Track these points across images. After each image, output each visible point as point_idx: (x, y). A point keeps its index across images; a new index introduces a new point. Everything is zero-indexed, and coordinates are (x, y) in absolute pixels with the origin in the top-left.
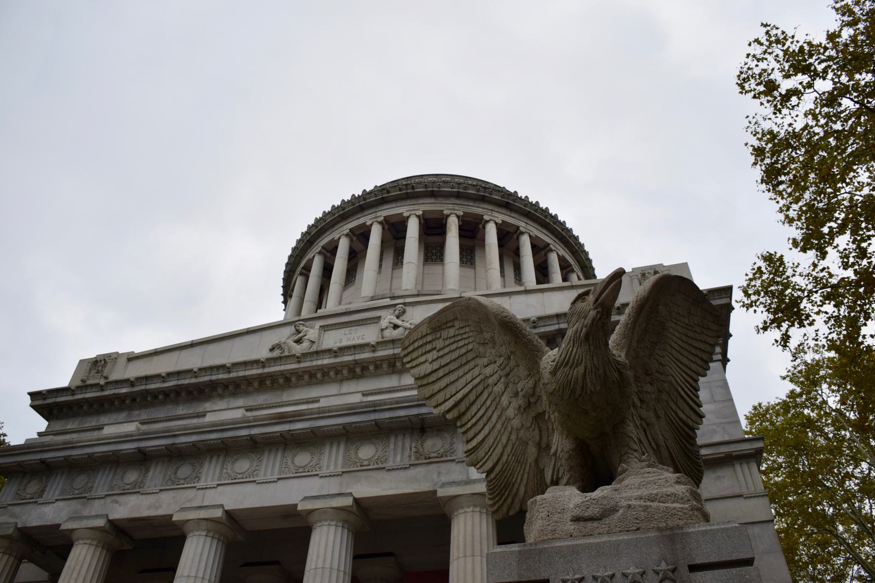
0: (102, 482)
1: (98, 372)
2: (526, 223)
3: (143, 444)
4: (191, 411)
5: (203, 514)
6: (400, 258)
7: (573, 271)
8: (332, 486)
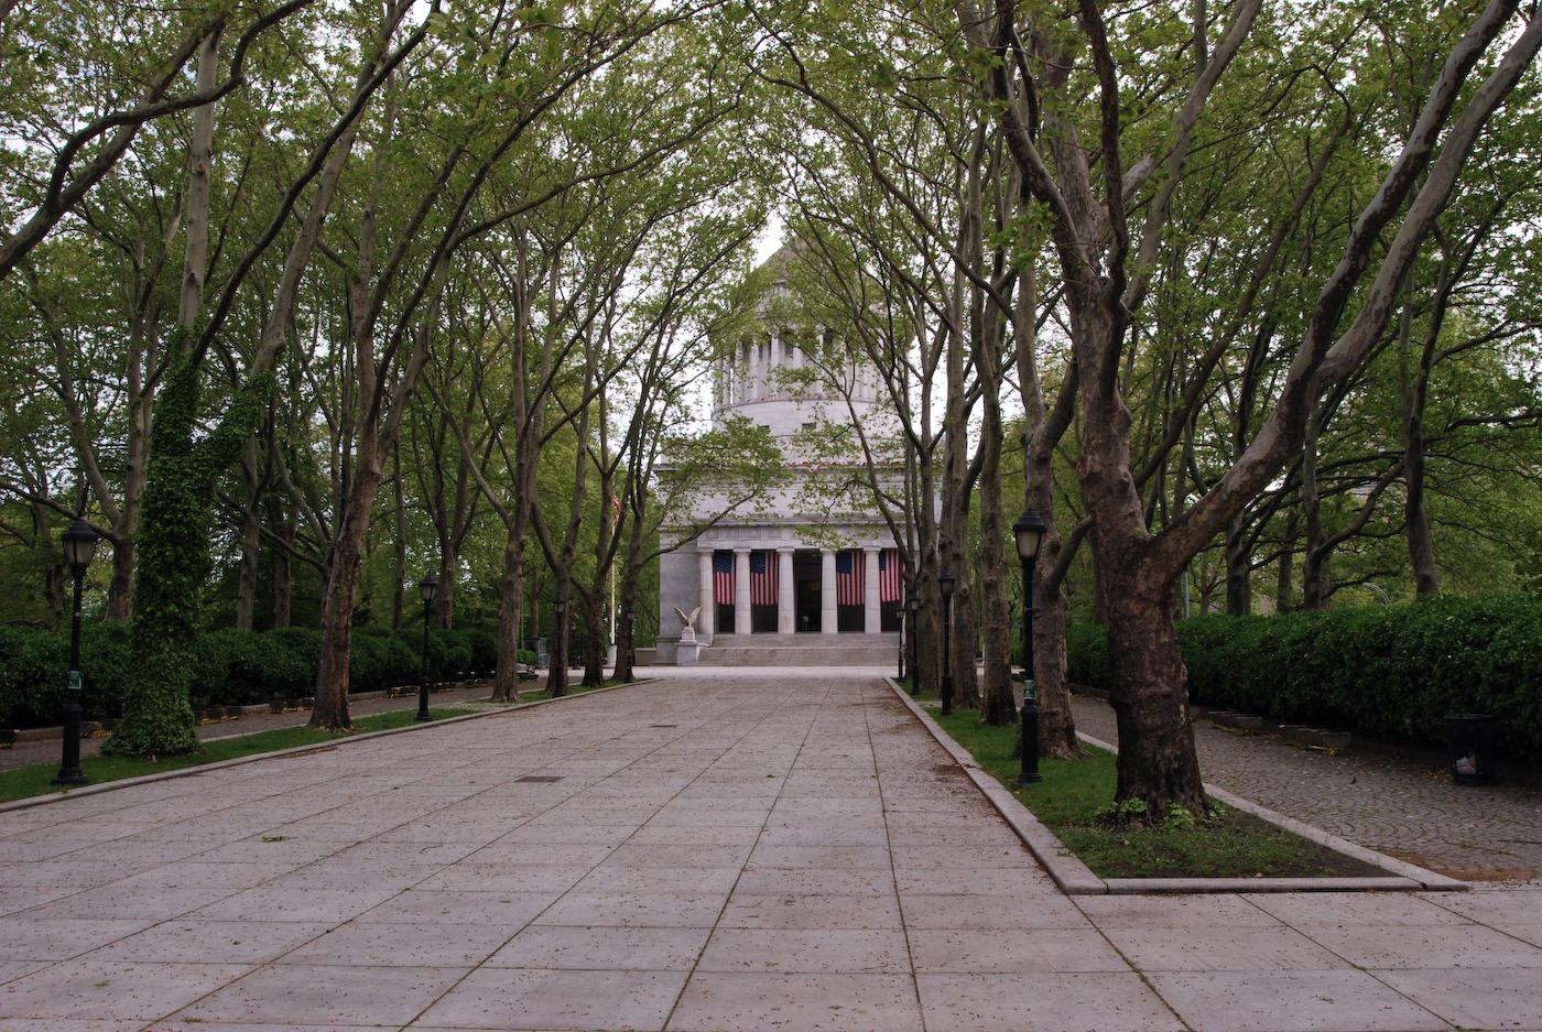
0: (742, 533)
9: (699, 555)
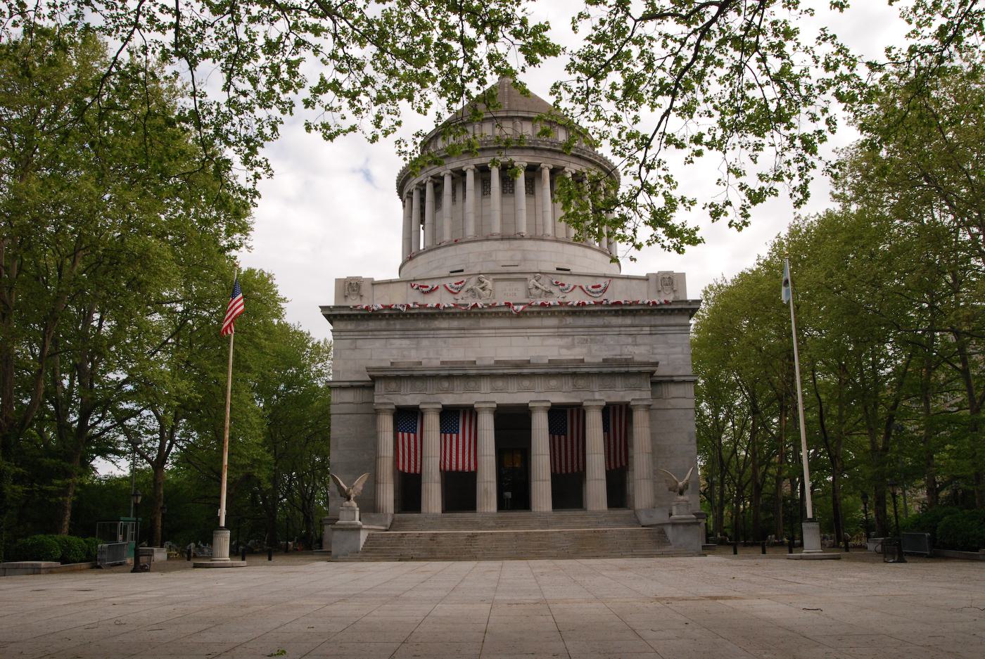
0: (430, 385)
1: (354, 290)
3: (451, 372)
4: (427, 326)
5: (488, 405)
9: (377, 412)
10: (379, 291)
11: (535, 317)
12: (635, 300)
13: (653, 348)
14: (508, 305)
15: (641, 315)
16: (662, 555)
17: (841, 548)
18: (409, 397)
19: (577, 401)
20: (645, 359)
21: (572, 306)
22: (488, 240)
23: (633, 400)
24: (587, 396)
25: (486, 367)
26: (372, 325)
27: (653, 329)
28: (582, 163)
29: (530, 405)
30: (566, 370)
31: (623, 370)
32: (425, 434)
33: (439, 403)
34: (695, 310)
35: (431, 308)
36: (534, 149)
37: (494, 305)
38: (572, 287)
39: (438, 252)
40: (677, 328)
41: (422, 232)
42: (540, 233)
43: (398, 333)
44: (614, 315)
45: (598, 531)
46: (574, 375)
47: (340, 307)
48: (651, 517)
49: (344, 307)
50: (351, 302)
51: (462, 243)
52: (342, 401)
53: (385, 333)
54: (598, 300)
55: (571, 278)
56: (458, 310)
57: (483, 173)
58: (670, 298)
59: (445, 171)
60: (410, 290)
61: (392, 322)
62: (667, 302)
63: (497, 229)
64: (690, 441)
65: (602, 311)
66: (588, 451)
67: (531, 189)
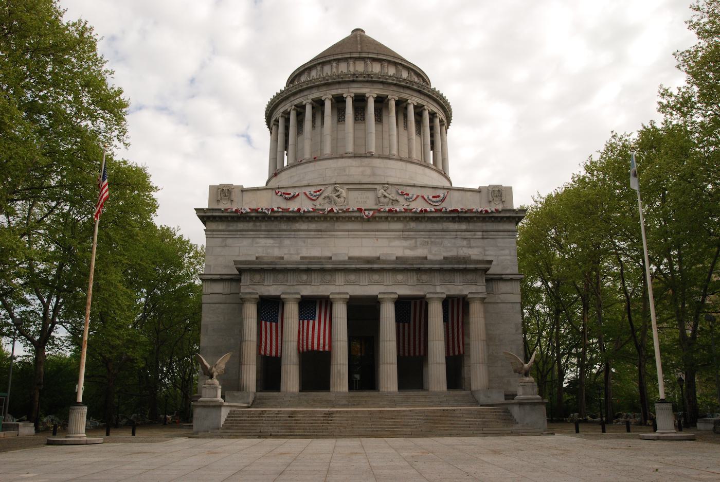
0: (291, 277)
2: (428, 102)
3: (310, 266)
4: (289, 228)
5: (342, 296)
6: (357, 114)
7: (444, 125)
8: (390, 290)
9: (243, 301)
10: (247, 196)
11: (383, 222)
12: (469, 208)
13: (485, 250)
14: (360, 210)
15: (474, 222)
16: (512, 433)
17: (649, 425)
18: (271, 289)
19: (422, 293)
20: (481, 258)
21: (415, 212)
22: (342, 157)
23: (469, 293)
24: (431, 289)
25: (343, 262)
26: (241, 226)
27: (484, 234)
28: (422, 97)
29: (379, 296)
30: (411, 266)
31: (461, 266)
32: (285, 320)
33: (299, 293)
34: (520, 219)
35: (293, 212)
36: (382, 83)
37: (347, 211)
38: (415, 197)
39: (299, 167)
40: (506, 233)
41: (286, 157)
42: (387, 153)
43: (263, 233)
44: (450, 222)
45: (447, 410)
46: (419, 271)
47: (213, 209)
48: (489, 397)
49: (216, 209)
50: (223, 206)
51: (320, 160)
52: (211, 291)
53: (252, 233)
54: (438, 208)
55: (414, 189)
56: (316, 214)
57: (339, 102)
58: (500, 207)
59: (307, 99)
60: (275, 197)
61: (258, 224)
62: (497, 211)
63: (350, 148)
64: (516, 331)
65: (441, 218)
66: (430, 337)
67: (379, 118)
